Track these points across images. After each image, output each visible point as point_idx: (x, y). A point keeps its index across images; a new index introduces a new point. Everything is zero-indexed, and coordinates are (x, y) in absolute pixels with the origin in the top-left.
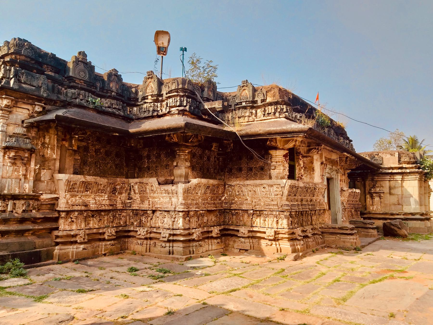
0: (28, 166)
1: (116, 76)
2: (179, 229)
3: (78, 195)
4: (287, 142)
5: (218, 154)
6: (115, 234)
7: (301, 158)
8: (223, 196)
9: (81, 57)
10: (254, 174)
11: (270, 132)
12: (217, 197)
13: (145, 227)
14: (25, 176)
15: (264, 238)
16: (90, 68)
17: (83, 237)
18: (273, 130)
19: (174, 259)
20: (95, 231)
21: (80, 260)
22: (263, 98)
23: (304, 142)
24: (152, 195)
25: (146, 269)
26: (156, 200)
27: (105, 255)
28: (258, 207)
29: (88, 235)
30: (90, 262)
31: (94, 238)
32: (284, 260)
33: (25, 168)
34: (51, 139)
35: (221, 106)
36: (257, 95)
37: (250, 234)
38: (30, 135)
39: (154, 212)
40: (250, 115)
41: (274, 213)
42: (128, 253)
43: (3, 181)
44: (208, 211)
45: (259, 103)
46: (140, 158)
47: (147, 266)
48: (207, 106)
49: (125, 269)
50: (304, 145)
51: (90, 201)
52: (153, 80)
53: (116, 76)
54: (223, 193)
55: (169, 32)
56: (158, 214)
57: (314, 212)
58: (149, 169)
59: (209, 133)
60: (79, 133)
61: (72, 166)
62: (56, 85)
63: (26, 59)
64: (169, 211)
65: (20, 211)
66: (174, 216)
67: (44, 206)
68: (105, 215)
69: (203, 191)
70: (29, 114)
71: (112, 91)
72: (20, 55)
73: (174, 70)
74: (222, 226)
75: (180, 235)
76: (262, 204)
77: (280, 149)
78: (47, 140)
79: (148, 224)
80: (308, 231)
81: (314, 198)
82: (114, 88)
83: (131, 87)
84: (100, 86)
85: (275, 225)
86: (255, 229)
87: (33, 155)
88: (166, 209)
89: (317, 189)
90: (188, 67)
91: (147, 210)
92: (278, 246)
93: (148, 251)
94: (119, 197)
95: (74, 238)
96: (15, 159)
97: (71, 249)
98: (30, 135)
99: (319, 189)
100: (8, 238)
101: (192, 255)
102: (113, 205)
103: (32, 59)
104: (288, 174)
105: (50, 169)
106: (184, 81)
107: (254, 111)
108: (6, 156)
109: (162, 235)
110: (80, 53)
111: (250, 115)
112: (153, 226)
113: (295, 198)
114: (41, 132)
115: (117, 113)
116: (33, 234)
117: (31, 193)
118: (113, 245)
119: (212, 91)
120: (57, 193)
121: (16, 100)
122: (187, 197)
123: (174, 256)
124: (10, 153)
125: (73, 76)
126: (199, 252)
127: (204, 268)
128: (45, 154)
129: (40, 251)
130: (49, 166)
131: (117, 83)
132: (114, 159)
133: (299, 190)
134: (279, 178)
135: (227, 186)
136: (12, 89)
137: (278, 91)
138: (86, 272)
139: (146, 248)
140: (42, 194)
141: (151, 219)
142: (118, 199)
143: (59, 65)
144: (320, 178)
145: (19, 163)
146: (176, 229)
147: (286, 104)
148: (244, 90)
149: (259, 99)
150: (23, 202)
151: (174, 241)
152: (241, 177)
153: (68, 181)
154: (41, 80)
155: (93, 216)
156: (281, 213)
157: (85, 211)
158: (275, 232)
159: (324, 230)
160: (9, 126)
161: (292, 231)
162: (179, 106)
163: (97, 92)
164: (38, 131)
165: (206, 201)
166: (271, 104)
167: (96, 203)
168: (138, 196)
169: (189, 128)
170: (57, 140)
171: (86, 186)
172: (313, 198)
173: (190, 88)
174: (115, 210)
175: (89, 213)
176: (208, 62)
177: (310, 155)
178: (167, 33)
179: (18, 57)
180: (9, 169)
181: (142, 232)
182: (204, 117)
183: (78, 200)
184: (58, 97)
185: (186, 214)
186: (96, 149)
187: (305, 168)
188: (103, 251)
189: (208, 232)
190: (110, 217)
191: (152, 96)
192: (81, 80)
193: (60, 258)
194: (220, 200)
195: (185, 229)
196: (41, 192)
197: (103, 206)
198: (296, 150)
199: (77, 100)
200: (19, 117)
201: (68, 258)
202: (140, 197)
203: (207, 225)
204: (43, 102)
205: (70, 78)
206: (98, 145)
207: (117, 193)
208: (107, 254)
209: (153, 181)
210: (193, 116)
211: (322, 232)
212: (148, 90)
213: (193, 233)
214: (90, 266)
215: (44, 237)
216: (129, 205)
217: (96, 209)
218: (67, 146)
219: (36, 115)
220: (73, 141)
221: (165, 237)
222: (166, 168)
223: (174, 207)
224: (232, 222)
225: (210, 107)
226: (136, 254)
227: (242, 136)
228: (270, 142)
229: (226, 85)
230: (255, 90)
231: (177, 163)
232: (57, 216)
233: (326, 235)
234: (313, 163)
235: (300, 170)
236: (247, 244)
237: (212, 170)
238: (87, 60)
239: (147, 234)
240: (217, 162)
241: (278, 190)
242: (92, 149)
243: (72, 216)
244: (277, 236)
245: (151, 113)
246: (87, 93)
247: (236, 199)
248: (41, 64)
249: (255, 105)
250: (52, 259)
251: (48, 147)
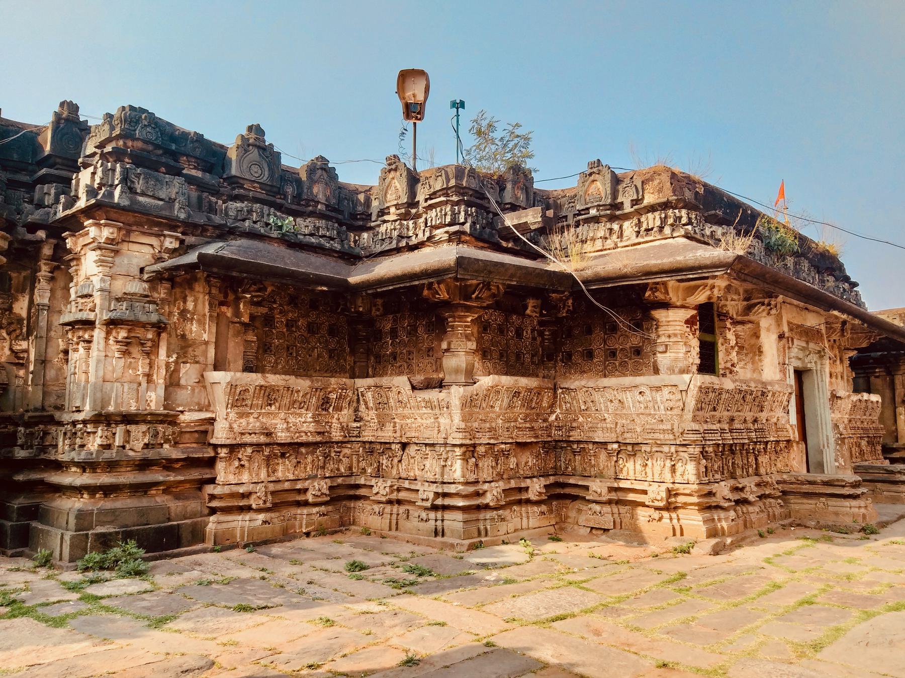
0: (153, 358)
1: (325, 169)
2: (454, 483)
3: (252, 414)
4: (692, 291)
5: (541, 323)
6: (328, 492)
7: (729, 325)
8: (552, 412)
9: (253, 135)
10: (620, 364)
11: (648, 269)
12: (538, 415)
13: (388, 477)
14: (149, 376)
15: (643, 505)
16: (270, 155)
17: (263, 498)
18: (655, 265)
19: (444, 546)
20: (287, 485)
21: (257, 544)
22: (635, 197)
23: (736, 289)
24: (400, 410)
25: (383, 565)
26: (409, 421)
27: (308, 534)
29: (273, 493)
30: (276, 549)
31: (285, 500)
32: (689, 553)
33: (148, 361)
34: (198, 302)
35: (540, 219)
36: (621, 190)
37: (613, 496)
38: (156, 295)
39: (404, 446)
40: (607, 235)
41: (666, 449)
42: (355, 532)
43: (105, 386)
44: (519, 444)
45: (628, 209)
46: (378, 335)
47: (388, 559)
48: (510, 220)
49: (341, 565)
50: (735, 297)
51: (277, 424)
52: (398, 173)
53: (325, 169)
54: (552, 406)
55: (426, 71)
56: (412, 450)
57: (762, 447)
58: (395, 358)
59: (512, 276)
60: (252, 289)
61: (241, 356)
62: (205, 194)
63: (145, 146)
64: (433, 445)
65: (138, 446)
66: (444, 456)
67: (187, 436)
68: (307, 453)
69: (506, 401)
70: (153, 256)
71: (318, 202)
72: (134, 139)
73: (439, 150)
74: (551, 478)
75: (457, 495)
76: (639, 430)
77: (677, 307)
78: (190, 305)
79: (394, 472)
80: (747, 489)
81: (763, 416)
82: (321, 197)
83: (356, 192)
84: (293, 192)
85: (668, 476)
86: (623, 484)
87: (164, 335)
88: (427, 441)
89: (770, 395)
90: (470, 140)
91: (389, 443)
92: (675, 521)
93: (394, 526)
94: (336, 416)
95: (245, 500)
96: (127, 344)
97: (240, 523)
98: (156, 295)
99: (773, 395)
100: (118, 500)
101: (483, 539)
102: (324, 433)
103: (157, 147)
104: (698, 361)
105: (197, 362)
106: (460, 172)
107: (616, 226)
108: (111, 338)
109: (421, 495)
110: (250, 128)
111: (607, 235)
112: (403, 475)
113: (713, 416)
114: (178, 290)
115: (328, 245)
116: (165, 492)
117: (161, 410)
118: (324, 515)
119: (522, 189)
120: (211, 409)
121: (128, 227)
122: (471, 415)
123: (445, 539)
124: (118, 333)
125: (238, 175)
126: (499, 533)
127: (505, 567)
128: (187, 333)
129: (178, 525)
130: (195, 356)
131: (326, 184)
132: (326, 341)
133: (723, 396)
134: (677, 370)
135: (560, 391)
136: (117, 207)
137: (668, 179)
138: (263, 570)
139: (390, 523)
140: (182, 412)
141: (400, 461)
142: (334, 421)
143: (212, 157)
144: (778, 370)
145: (135, 350)
146: (449, 483)
147: (688, 206)
148: (593, 181)
149: (626, 199)
150: (143, 427)
151: (445, 508)
152: (590, 370)
153: (232, 386)
154: (174, 188)
155: (283, 455)
156: (681, 449)
157: (267, 445)
158: (669, 491)
159: (787, 488)
160: (115, 279)
161: (707, 488)
162: (450, 225)
163: (287, 205)
164: (173, 287)
165: (512, 424)
166: (652, 208)
167: (288, 429)
168: (373, 413)
169: (465, 269)
170: (210, 305)
171: (269, 395)
172: (760, 414)
173: (474, 184)
174: (326, 442)
175: (275, 450)
176: (511, 128)
177: (751, 317)
178: (421, 73)
179: (130, 143)
180: (117, 363)
181: (382, 488)
182: (504, 244)
183: (252, 423)
184: (209, 219)
185: (470, 451)
186: (287, 320)
187: (741, 348)
188: (304, 526)
189: (520, 490)
190: (318, 457)
191: (397, 206)
192: (254, 181)
193: (218, 539)
194: (545, 420)
195: (467, 483)
196: (181, 409)
197: (303, 434)
198: (718, 308)
199: (247, 223)
200: (135, 261)
201: (234, 540)
202: (378, 416)
203: (518, 475)
204: (179, 230)
205: (235, 179)
206: (292, 312)
207: (331, 408)
208: (313, 534)
209: (401, 382)
210: (481, 244)
211: (784, 493)
212: (388, 196)
213: (486, 491)
214: (274, 557)
215: (187, 498)
216: (356, 433)
217: (289, 441)
218: (229, 315)
219: (166, 256)
220: (241, 306)
221: (427, 500)
222: (428, 356)
223: (444, 436)
224: (574, 469)
225: (516, 222)
226: (370, 534)
227: (587, 282)
228: (653, 293)
229: (553, 175)
230: (616, 181)
231: (449, 344)
232: (212, 454)
233: (792, 499)
234: (758, 337)
235: (728, 353)
236: (606, 516)
237: (527, 358)
238: (264, 141)
239: (392, 492)
240: (539, 339)
241: (672, 397)
242: (280, 320)
243: (240, 456)
244: (673, 500)
245: (394, 242)
246: (266, 208)
247: (581, 419)
248: (175, 155)
249: (618, 213)
250: (203, 541)
251: (193, 318)
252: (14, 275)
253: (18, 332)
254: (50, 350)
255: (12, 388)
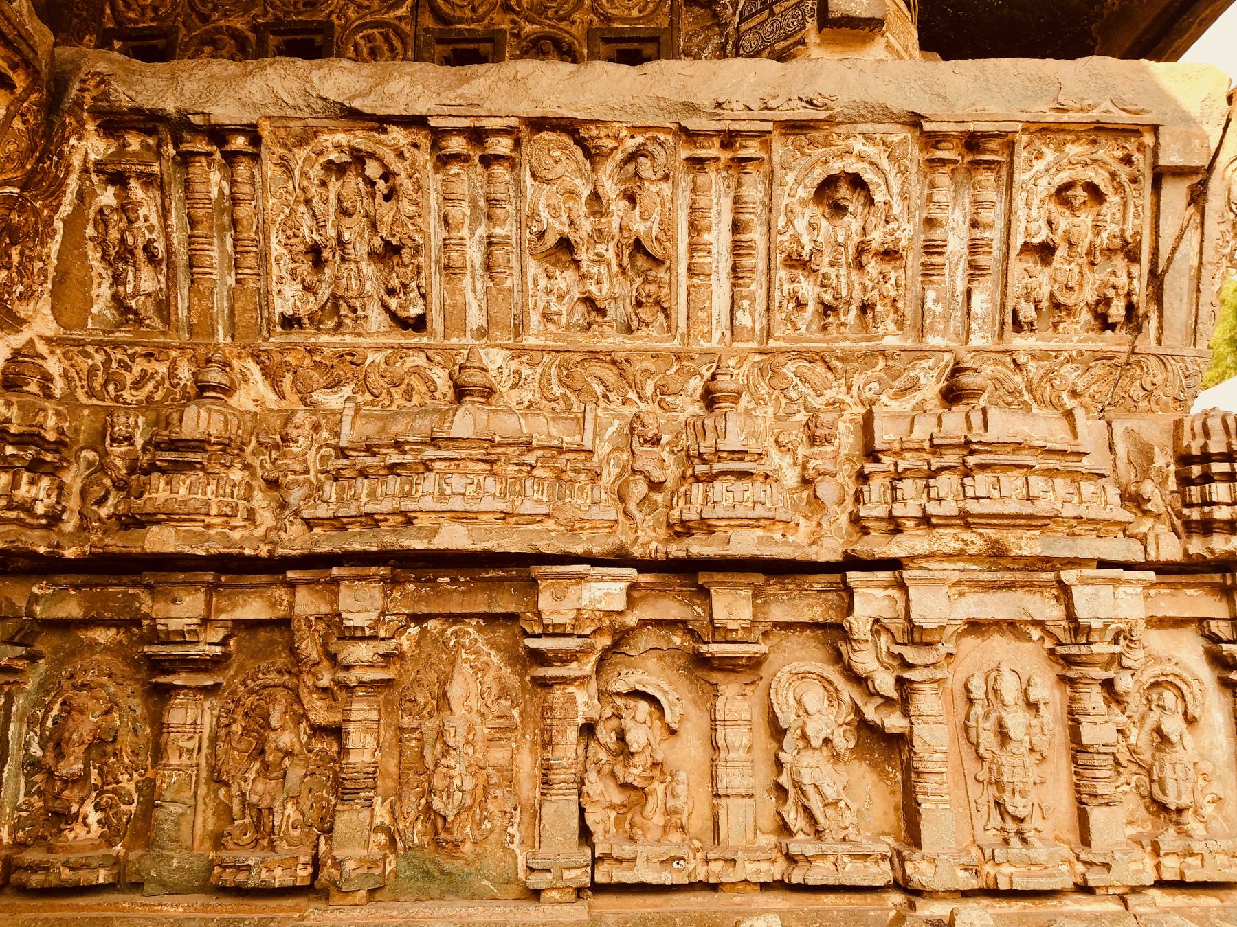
28: (728, 497)
135: (93, 146)
224: (143, 827)
247: (254, 393)
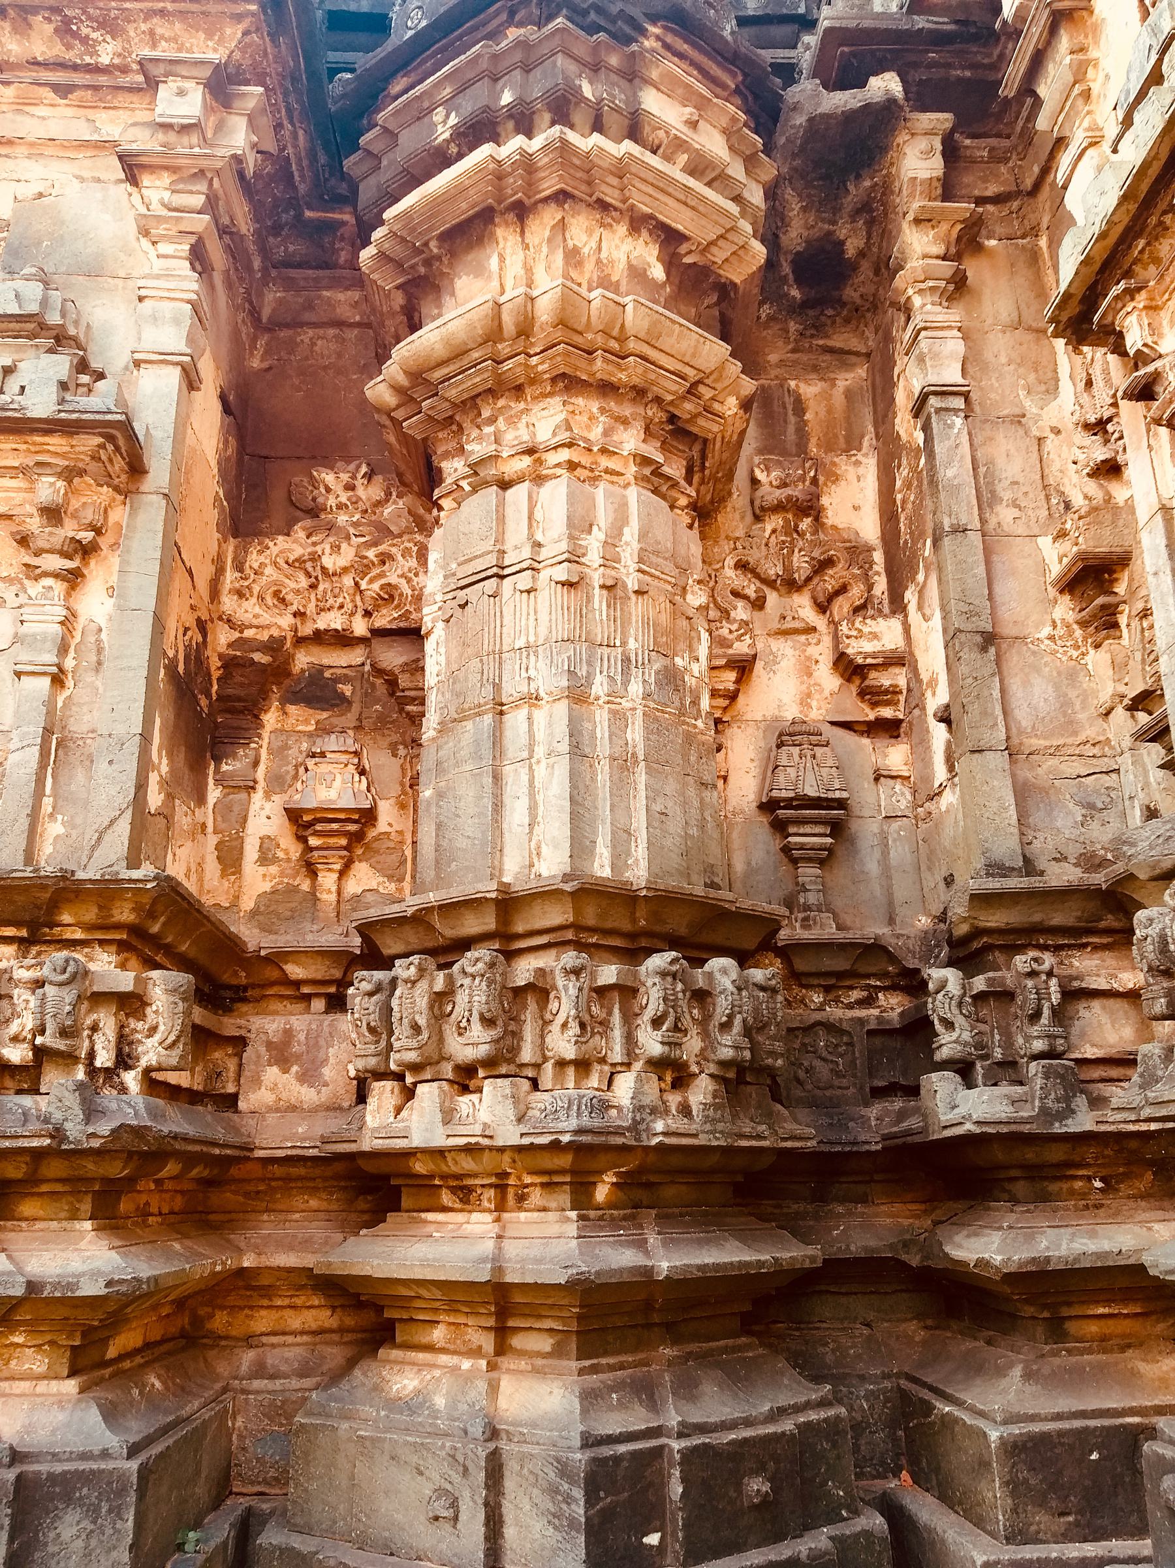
252: (810, 390)
253: (856, 592)
254: (1006, 589)
255: (867, 829)
